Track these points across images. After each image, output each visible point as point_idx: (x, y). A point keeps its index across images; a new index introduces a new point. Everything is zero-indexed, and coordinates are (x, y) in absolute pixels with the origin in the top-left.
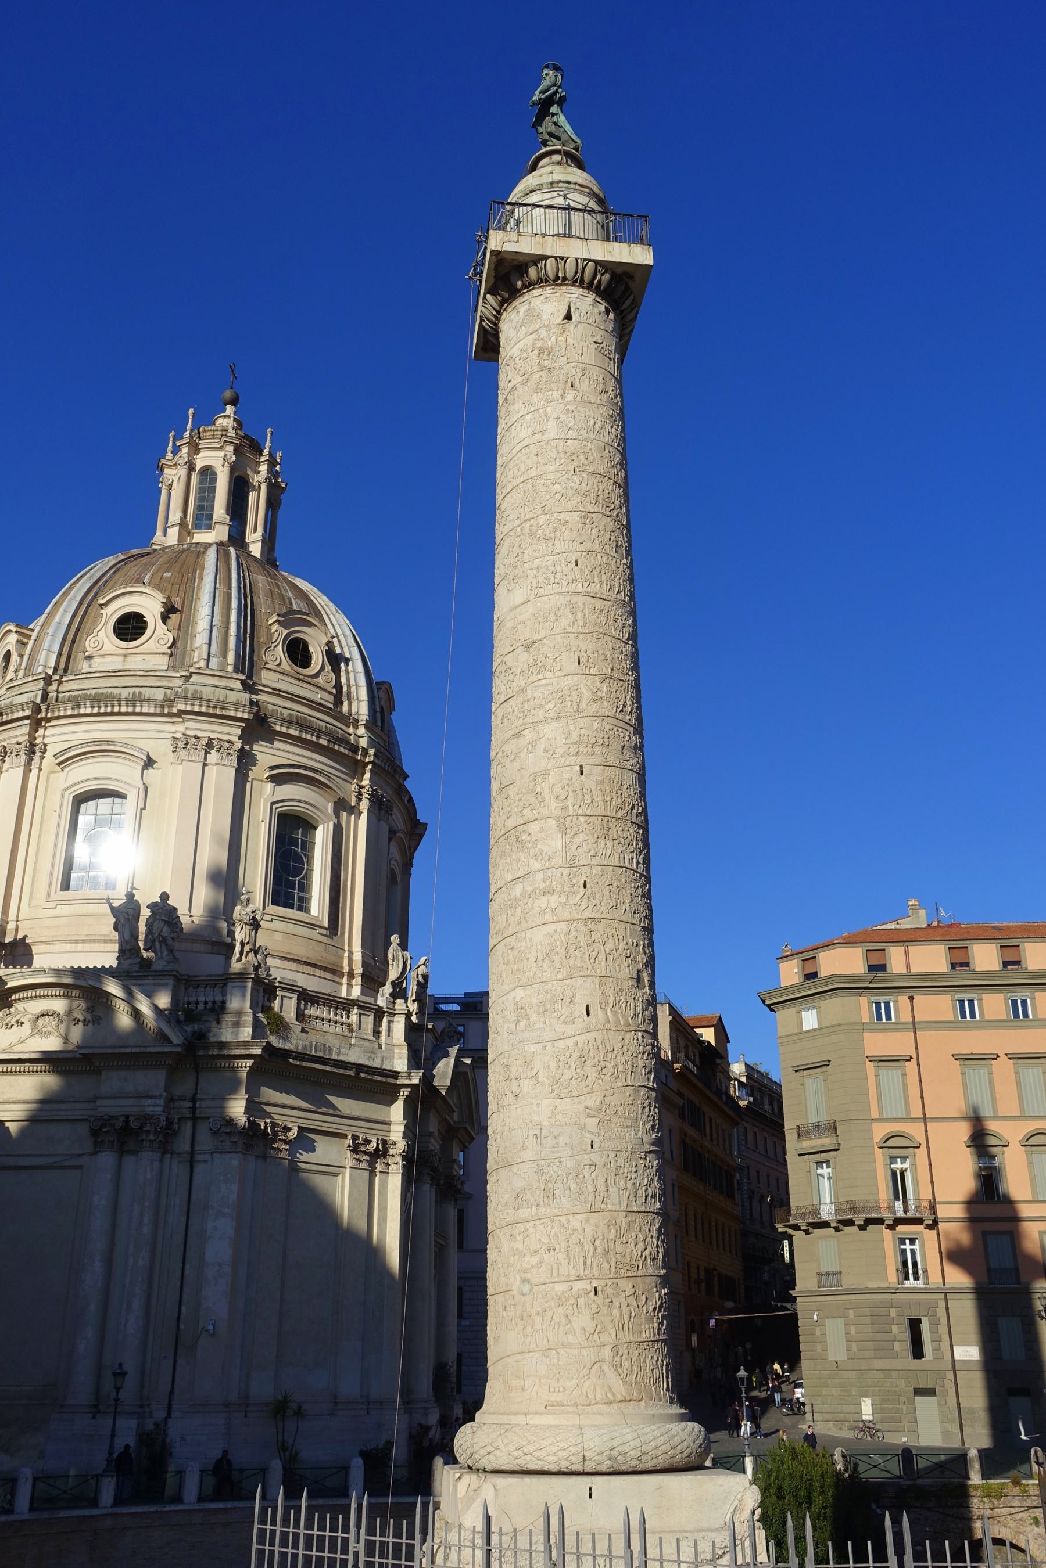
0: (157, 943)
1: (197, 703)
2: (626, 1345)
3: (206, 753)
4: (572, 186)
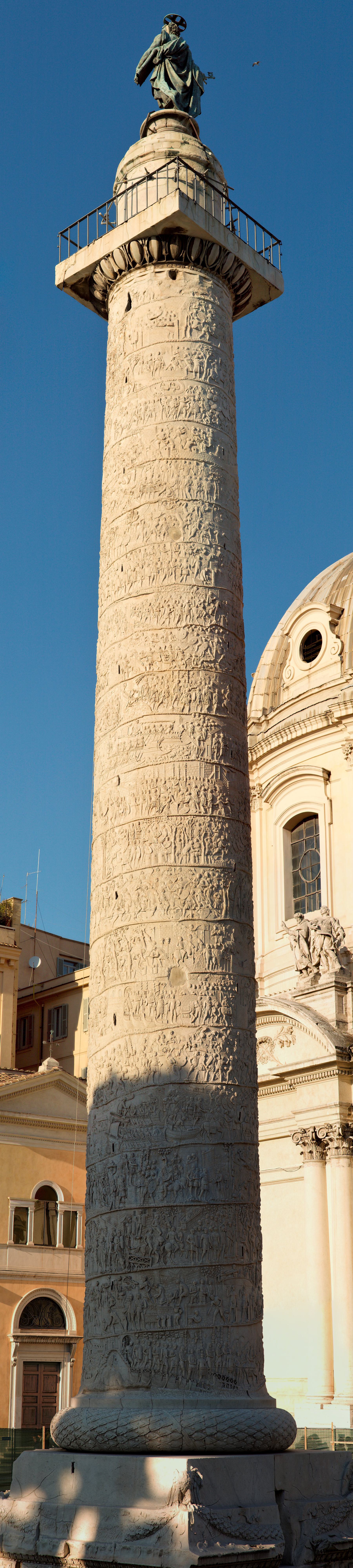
0: (323, 958)
2: (137, 1335)
4: (137, 162)
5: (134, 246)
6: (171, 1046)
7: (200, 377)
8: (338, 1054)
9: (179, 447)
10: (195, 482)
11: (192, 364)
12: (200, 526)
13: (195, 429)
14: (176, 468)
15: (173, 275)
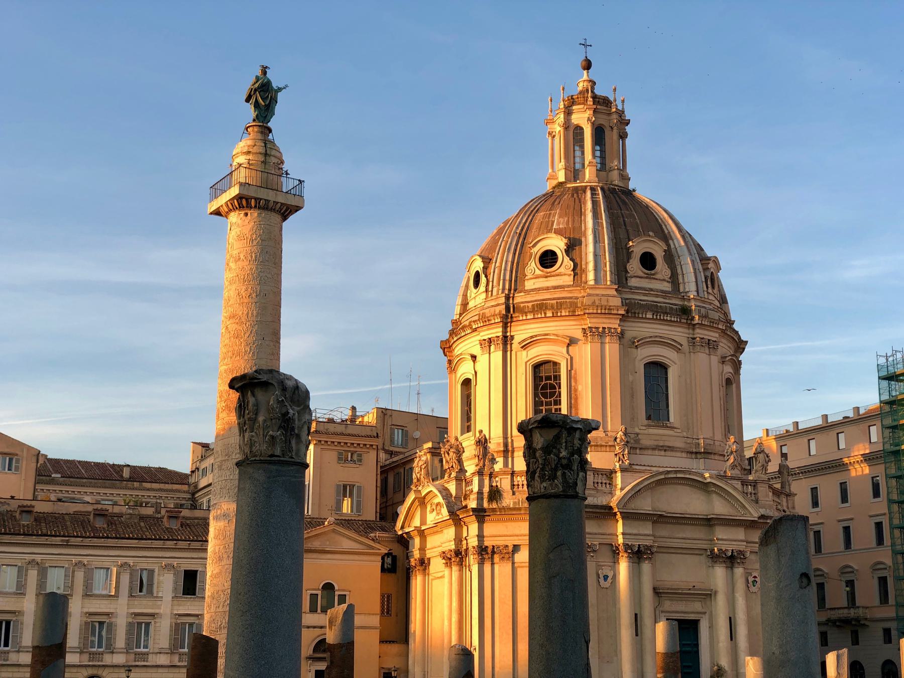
1: (478, 322)
3: (490, 346)
4: (236, 156)
5: (228, 202)
6: (227, 550)
7: (255, 262)
8: (450, 515)
9: (244, 297)
10: (250, 312)
11: (252, 257)
12: (251, 332)
13: (252, 288)
14: (242, 307)
15: (246, 214)
